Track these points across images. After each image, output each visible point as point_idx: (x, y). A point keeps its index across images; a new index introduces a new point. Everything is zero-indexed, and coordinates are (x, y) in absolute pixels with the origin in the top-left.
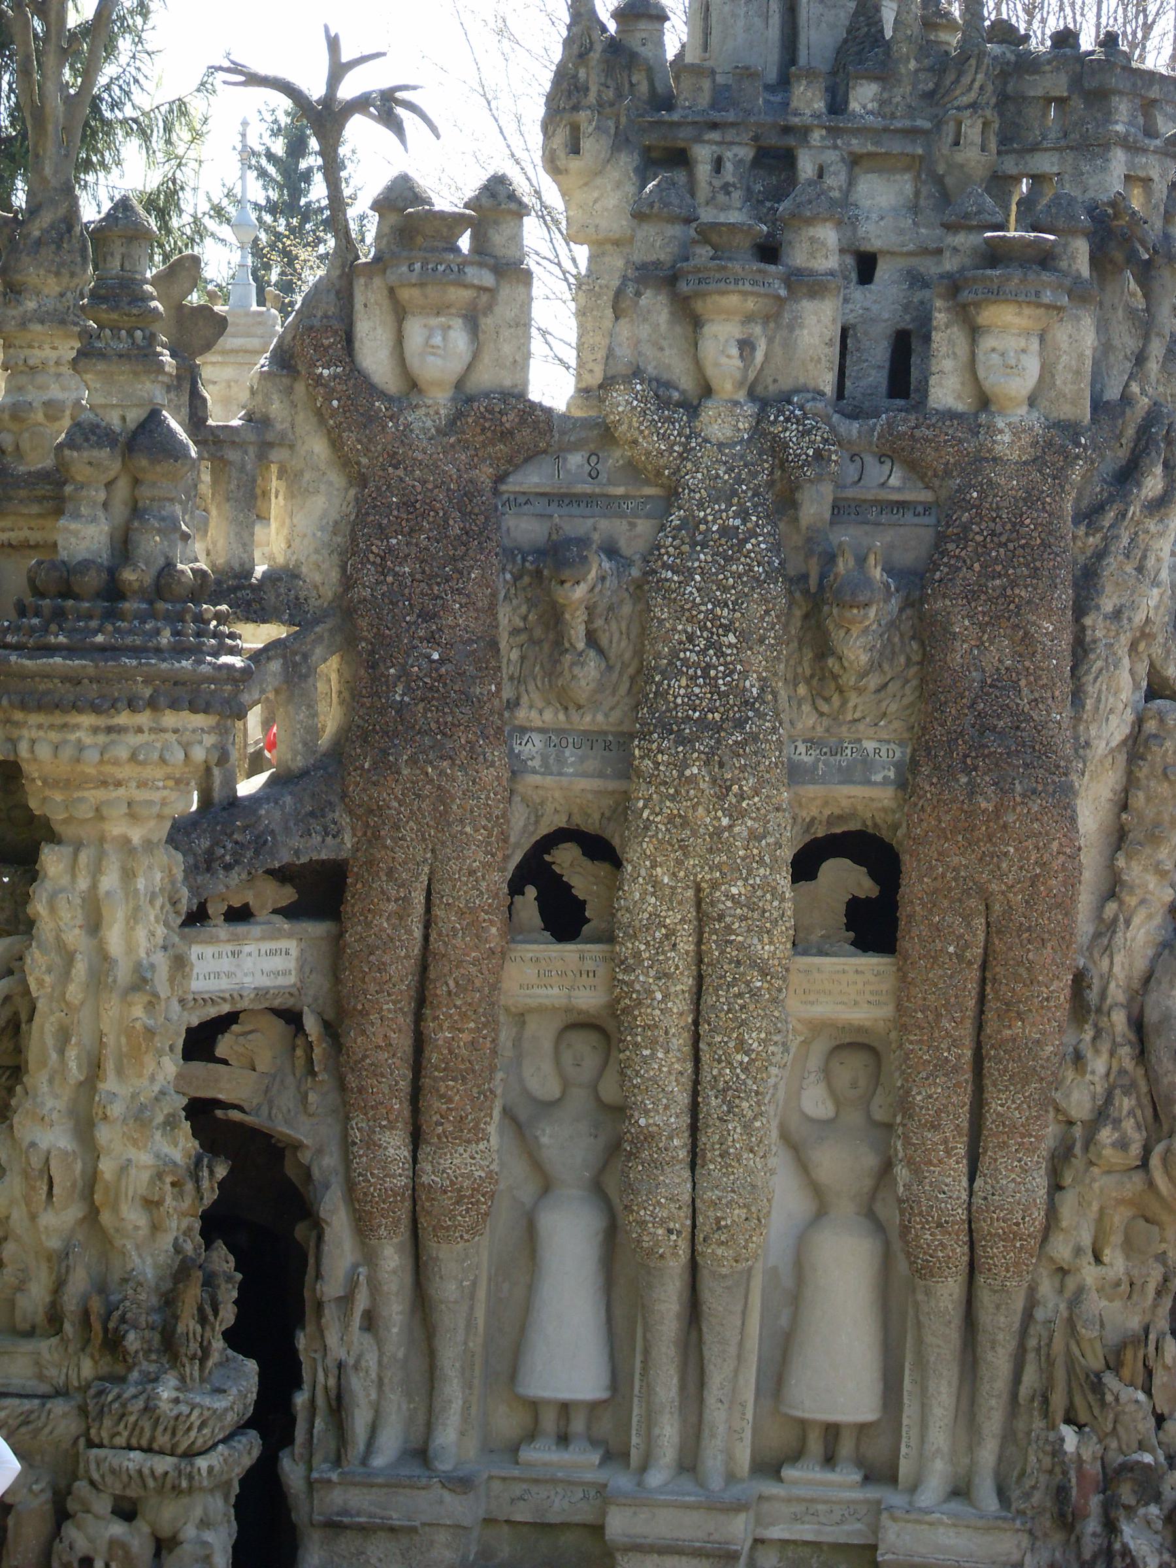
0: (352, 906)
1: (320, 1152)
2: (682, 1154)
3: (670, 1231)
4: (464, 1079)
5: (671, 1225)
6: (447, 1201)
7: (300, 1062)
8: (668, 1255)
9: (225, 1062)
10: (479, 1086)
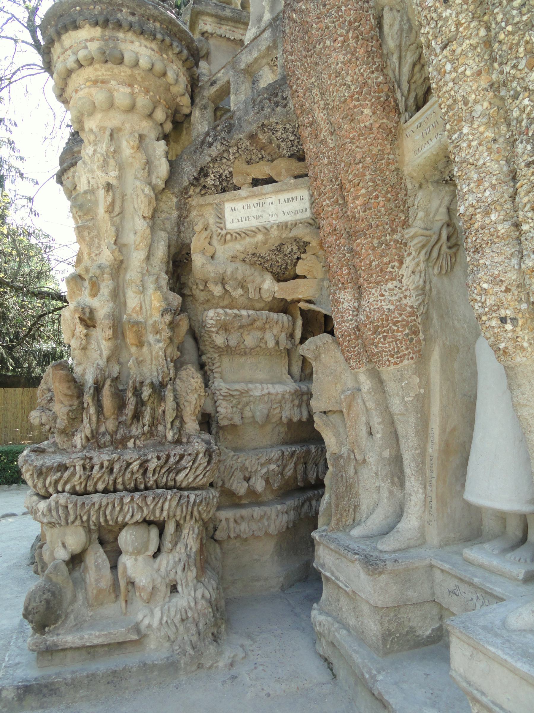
2: (503, 228)
3: (503, 320)
4: (365, 235)
5: (502, 313)
8: (511, 350)
10: (379, 238)
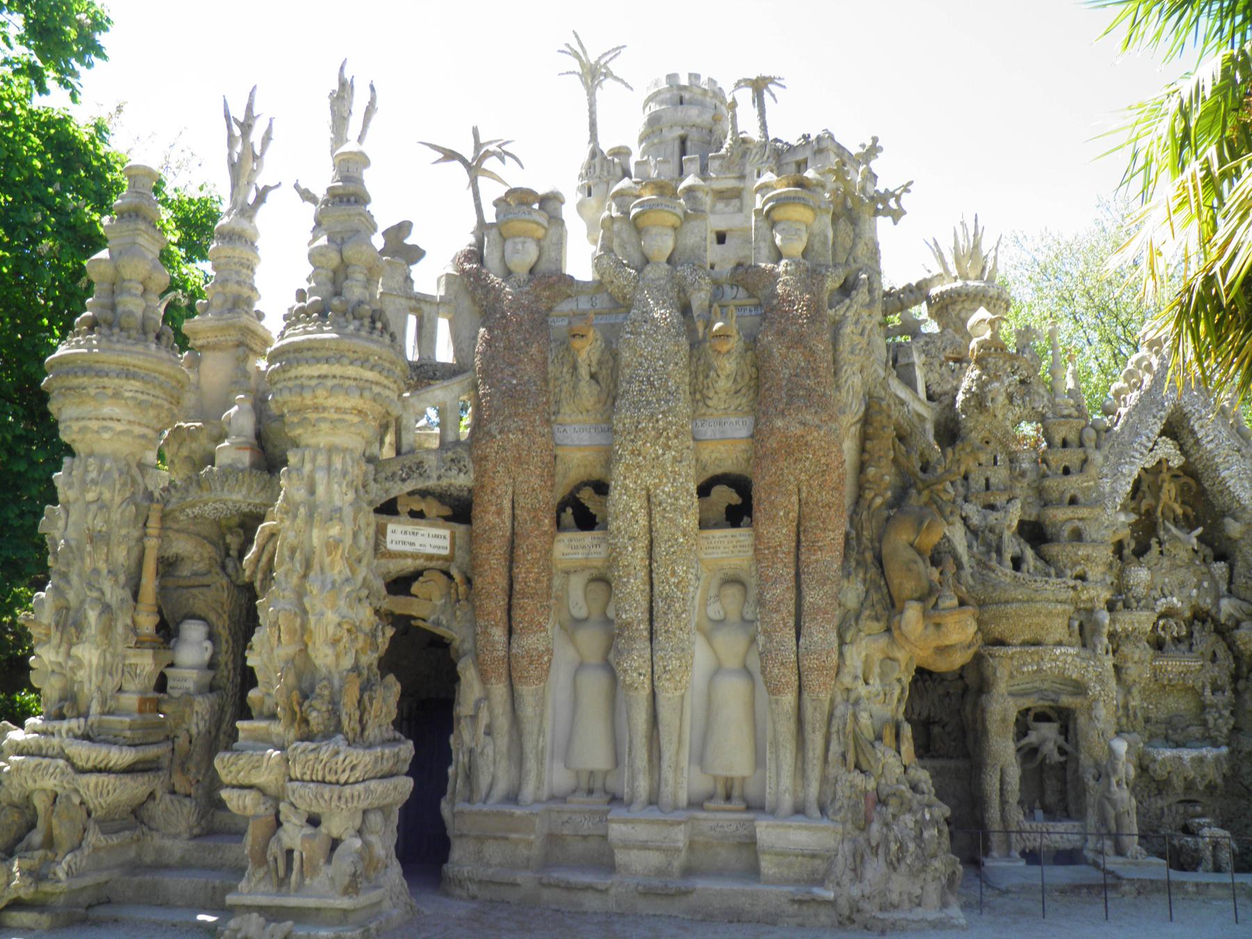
0: (476, 512)
1: (463, 641)
2: (645, 633)
6: (525, 662)
7: (454, 596)
9: (416, 596)
